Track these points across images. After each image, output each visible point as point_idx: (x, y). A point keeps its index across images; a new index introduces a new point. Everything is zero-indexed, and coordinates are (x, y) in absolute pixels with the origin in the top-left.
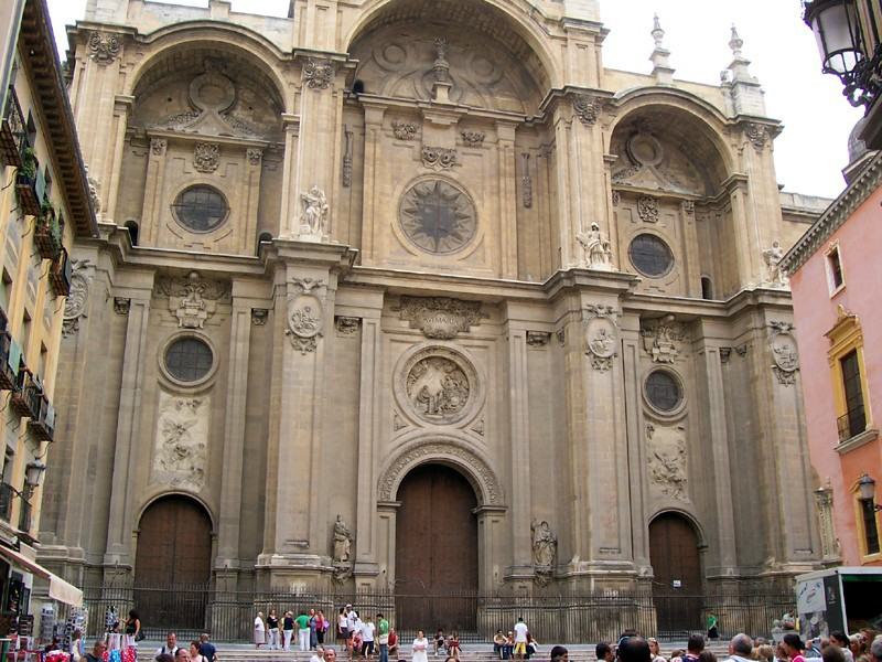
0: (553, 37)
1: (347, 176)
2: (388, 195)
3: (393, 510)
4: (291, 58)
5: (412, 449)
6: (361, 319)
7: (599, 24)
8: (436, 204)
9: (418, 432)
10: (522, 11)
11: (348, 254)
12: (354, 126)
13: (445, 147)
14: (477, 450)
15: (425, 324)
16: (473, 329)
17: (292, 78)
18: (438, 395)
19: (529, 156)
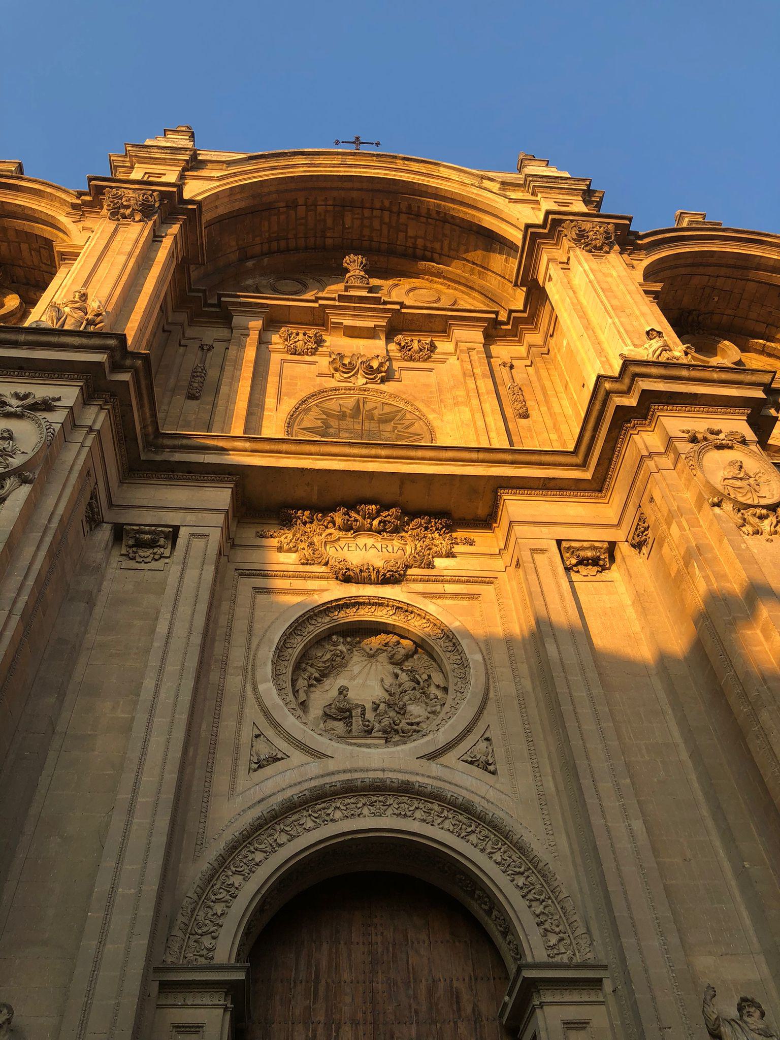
0: (517, 201)
1: (196, 385)
2: (271, 410)
3: (218, 999)
4: (88, 198)
5: (290, 808)
6: (176, 529)
7: (585, 180)
8: (358, 427)
9: (314, 768)
10: (463, 184)
11: (128, 362)
12: (215, 340)
13: (369, 356)
14: (480, 804)
15: (331, 551)
16: (438, 562)
17: (88, 223)
18: (376, 707)
19: (512, 367)
